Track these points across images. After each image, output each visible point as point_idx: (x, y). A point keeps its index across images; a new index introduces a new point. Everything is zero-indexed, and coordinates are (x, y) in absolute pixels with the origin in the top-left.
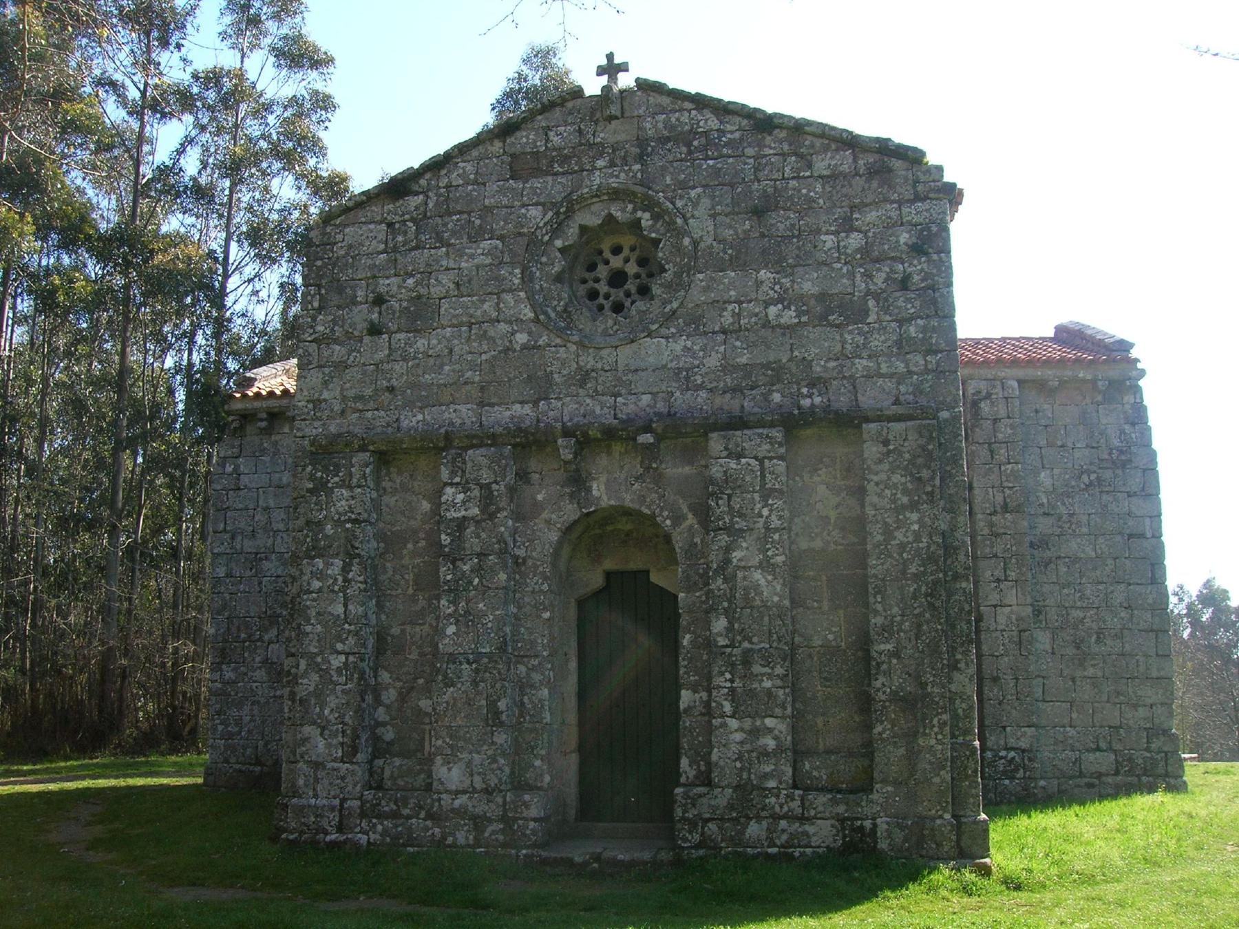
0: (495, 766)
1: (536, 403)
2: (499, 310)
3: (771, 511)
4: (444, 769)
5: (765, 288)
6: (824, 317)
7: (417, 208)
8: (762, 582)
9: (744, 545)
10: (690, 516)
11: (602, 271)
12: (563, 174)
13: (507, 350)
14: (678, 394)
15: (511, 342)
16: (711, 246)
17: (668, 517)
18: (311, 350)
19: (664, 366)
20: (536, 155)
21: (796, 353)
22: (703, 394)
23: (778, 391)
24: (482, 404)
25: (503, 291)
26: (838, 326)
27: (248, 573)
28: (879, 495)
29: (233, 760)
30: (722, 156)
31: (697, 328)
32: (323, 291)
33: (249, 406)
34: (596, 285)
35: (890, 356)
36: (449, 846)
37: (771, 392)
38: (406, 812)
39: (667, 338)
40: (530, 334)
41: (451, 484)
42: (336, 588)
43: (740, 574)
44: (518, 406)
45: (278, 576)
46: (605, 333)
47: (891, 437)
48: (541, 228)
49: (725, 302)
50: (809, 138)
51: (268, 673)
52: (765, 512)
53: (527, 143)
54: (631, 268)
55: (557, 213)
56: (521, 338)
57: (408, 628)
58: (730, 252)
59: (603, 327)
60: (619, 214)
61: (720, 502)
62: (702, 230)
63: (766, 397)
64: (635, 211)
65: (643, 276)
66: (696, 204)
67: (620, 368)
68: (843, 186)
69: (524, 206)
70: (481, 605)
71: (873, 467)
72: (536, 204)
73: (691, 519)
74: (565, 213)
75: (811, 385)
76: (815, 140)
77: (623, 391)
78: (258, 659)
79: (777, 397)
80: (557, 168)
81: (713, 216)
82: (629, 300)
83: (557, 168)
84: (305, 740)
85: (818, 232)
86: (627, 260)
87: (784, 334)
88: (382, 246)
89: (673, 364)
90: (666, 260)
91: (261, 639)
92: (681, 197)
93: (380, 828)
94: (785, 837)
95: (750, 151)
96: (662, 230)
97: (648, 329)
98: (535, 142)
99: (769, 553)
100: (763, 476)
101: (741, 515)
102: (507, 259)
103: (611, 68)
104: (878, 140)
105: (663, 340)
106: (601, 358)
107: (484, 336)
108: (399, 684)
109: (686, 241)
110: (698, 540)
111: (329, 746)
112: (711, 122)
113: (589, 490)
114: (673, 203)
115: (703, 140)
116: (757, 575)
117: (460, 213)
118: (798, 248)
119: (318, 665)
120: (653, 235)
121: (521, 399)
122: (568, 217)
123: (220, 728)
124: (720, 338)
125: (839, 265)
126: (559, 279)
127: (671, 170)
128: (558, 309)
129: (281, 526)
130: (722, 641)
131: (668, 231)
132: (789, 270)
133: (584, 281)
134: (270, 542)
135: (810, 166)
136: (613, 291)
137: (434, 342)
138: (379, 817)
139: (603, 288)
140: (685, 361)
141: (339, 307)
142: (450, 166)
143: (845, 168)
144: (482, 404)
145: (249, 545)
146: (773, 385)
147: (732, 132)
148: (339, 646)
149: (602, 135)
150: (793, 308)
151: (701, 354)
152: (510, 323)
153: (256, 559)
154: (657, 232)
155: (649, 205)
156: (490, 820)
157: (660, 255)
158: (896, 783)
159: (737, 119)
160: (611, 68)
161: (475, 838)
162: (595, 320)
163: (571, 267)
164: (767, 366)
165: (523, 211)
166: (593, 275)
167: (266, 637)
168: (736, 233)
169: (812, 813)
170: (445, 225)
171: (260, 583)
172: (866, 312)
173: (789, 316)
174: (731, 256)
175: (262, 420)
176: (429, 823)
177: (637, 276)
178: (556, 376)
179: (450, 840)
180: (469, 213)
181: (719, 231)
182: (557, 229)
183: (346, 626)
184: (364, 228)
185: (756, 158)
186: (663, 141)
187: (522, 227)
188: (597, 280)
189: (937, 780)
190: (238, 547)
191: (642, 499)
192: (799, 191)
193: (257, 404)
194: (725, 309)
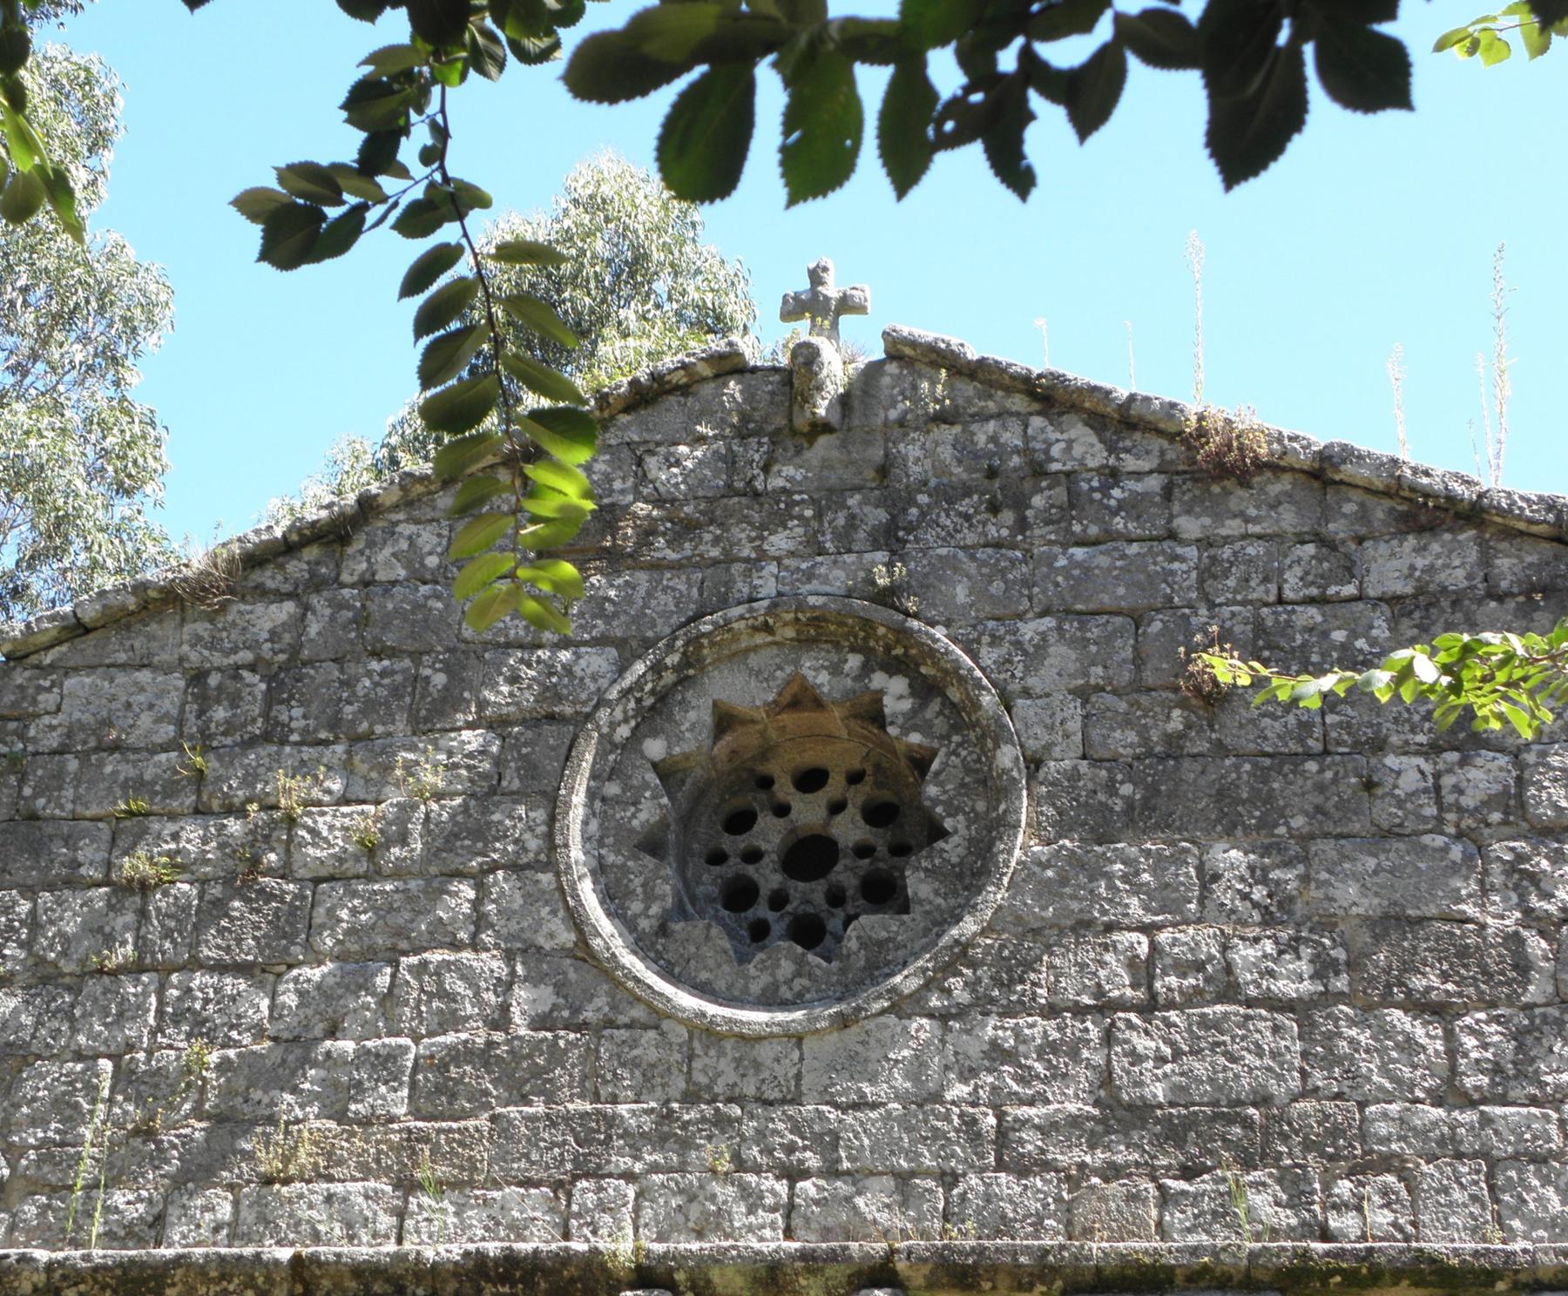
7: (274, 636)
11: (769, 834)
12: (676, 567)
30: (1110, 536)
40: (559, 988)
50: (1356, 495)
54: (849, 830)
55: (657, 668)
58: (1126, 789)
59: (765, 979)
60: (823, 678)
62: (1050, 728)
64: (866, 670)
65: (882, 850)
66: (1035, 655)
72: (600, 642)
74: (677, 669)
76: (1370, 500)
81: (1083, 694)
82: (840, 914)
86: (837, 808)
88: (168, 731)
90: (948, 804)
92: (995, 641)
95: (1190, 526)
96: (940, 725)
98: (608, 479)
102: (512, 782)
106: (757, 1066)
109: (1007, 756)
112: (1078, 446)
114: (975, 657)
115: (1060, 494)
118: (1321, 788)
120: (915, 738)
122: (683, 681)
125: (1440, 841)
126: (652, 845)
127: (972, 567)
128: (644, 924)
131: (956, 728)
133: (717, 858)
135: (1349, 570)
136: (797, 888)
139: (769, 877)
143: (1456, 577)
147: (1138, 475)
149: (789, 470)
150: (1306, 952)
154: (925, 729)
155: (903, 658)
157: (932, 790)
159: (1158, 443)
162: (743, 959)
163: (687, 820)
165: (565, 656)
166: (742, 842)
168: (1145, 740)
170: (349, 684)
174: (1129, 802)
177: (863, 851)
180: (416, 656)
181: (1096, 734)
184: (121, 678)
185: (1205, 543)
186: (948, 494)
187: (559, 698)
188: (753, 856)
192: (1325, 634)
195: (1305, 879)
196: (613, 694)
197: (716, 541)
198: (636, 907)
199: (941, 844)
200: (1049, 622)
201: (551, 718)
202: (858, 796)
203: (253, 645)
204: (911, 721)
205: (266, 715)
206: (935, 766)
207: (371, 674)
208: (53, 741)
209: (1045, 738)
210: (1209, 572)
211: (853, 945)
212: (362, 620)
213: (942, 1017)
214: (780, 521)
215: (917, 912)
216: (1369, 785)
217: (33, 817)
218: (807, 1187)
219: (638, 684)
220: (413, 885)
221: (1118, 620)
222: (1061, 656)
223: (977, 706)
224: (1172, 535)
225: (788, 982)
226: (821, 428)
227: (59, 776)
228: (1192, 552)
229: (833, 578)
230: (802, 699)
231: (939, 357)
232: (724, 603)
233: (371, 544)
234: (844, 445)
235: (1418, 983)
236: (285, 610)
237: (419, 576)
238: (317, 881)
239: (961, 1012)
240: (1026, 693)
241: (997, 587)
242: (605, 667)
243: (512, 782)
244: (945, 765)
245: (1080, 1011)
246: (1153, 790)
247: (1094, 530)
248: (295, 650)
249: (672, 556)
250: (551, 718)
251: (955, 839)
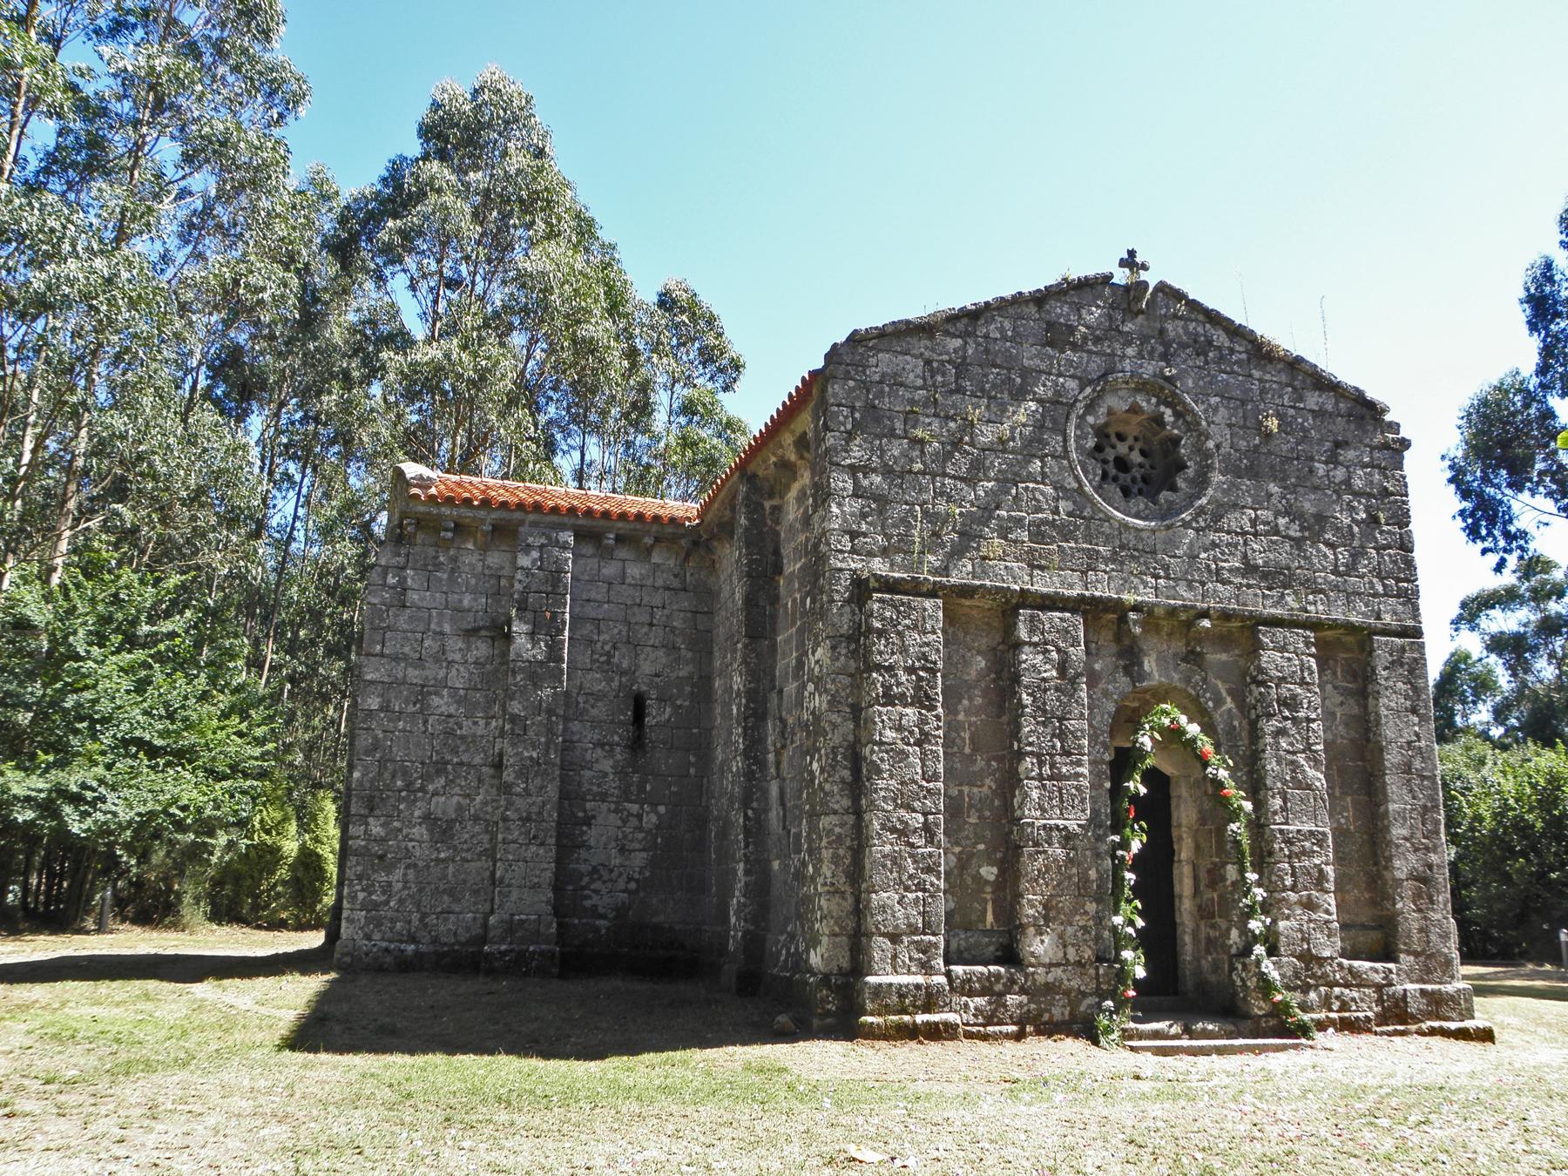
7: (955, 351)
10: (1229, 699)
12: (1096, 353)
27: (411, 709)
29: (377, 936)
30: (1232, 372)
32: (857, 415)
33: (434, 511)
40: (1075, 503)
41: (1030, 644)
45: (450, 716)
51: (431, 831)
54: (1136, 457)
57: (966, 789)
64: (1158, 404)
66: (1216, 410)
73: (1229, 703)
78: (417, 813)
80: (1090, 346)
81: (1230, 426)
84: (883, 908)
85: (1312, 459)
86: (1131, 449)
91: (423, 789)
95: (1256, 374)
102: (1048, 424)
103: (1130, 261)
104: (1357, 389)
108: (957, 850)
110: (1236, 723)
113: (1141, 664)
123: (361, 895)
129: (457, 657)
131: (1189, 430)
134: (442, 674)
135: (1301, 399)
136: (1122, 475)
143: (1329, 407)
145: (414, 675)
153: (422, 694)
155: (1173, 402)
156: (1084, 995)
158: (1416, 954)
160: (1130, 261)
167: (431, 788)
170: (986, 375)
171: (426, 722)
175: (446, 530)
177: (1141, 466)
179: (1046, 1017)
180: (1009, 370)
185: (1260, 380)
186: (1183, 346)
190: (400, 675)
193: (446, 511)
201: (1058, 402)
202: (1138, 446)
203: (948, 353)
204: (1174, 425)
208: (877, 378)
210: (1263, 391)
212: (987, 351)
213: (1197, 530)
214: (1129, 343)
216: (1311, 471)
217: (874, 407)
222: (1222, 411)
223: (1199, 424)
224: (1251, 376)
226: (1141, 312)
227: (882, 392)
229: (1149, 369)
230: (1135, 409)
231: (1178, 295)
236: (958, 342)
237: (1005, 338)
239: (1203, 529)
243: (1048, 424)
248: (964, 358)
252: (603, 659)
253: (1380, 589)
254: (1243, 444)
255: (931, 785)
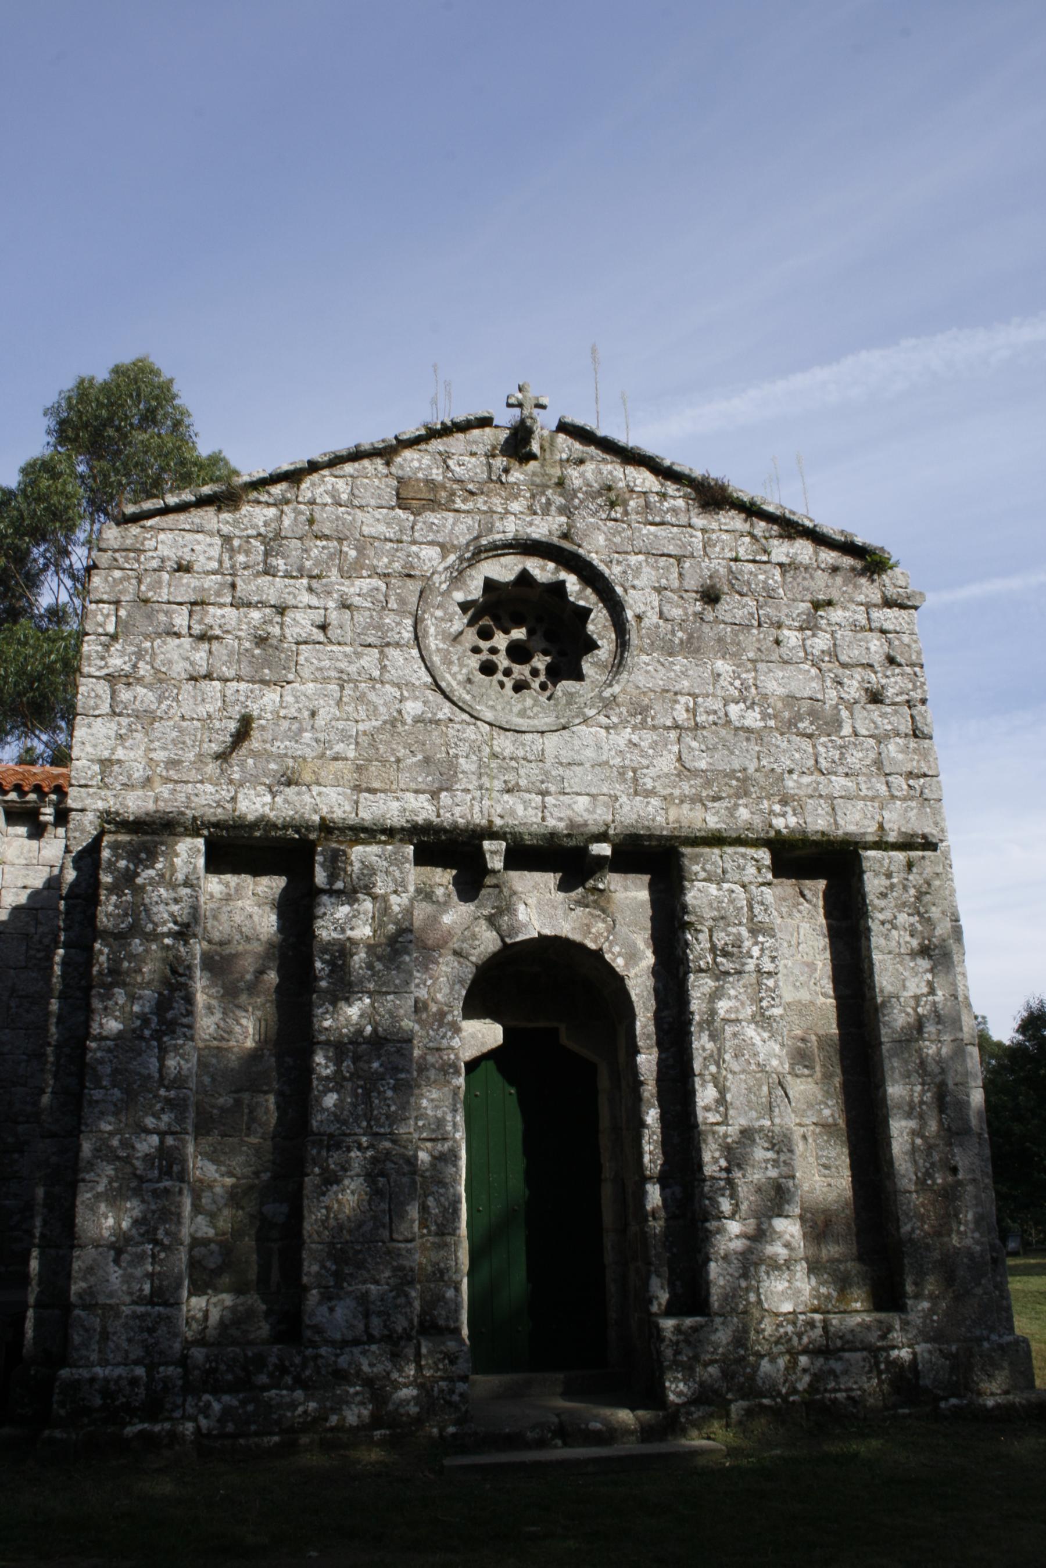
0: (401, 1300)
1: (435, 795)
2: (384, 668)
3: (762, 950)
4: (324, 1309)
5: (722, 682)
6: (792, 723)
8: (757, 1040)
9: (732, 992)
13: (393, 723)
14: (624, 799)
15: (400, 712)
16: (657, 626)
17: (620, 954)
18: (100, 692)
19: (607, 763)
20: (429, 482)
21: (764, 762)
22: (655, 801)
23: (746, 806)
24: (357, 788)
25: (388, 644)
26: (810, 736)
28: (887, 937)
31: (644, 721)
32: (122, 613)
34: (494, 657)
35: (869, 776)
36: (332, 1429)
37: (736, 806)
38: (263, 1379)
39: (607, 728)
42: (147, 1033)
43: (729, 1030)
44: (410, 796)
46: (522, 714)
47: (892, 868)
48: (440, 573)
49: (676, 694)
52: (756, 951)
53: (420, 468)
55: (461, 559)
56: (412, 708)
57: (246, 1096)
58: (680, 634)
59: (520, 706)
61: (701, 936)
62: (645, 604)
63: (732, 811)
66: (637, 571)
67: (550, 760)
68: (804, 579)
69: (414, 542)
70: (375, 1065)
71: (876, 902)
72: (431, 543)
74: (469, 559)
75: (784, 802)
77: (553, 789)
79: (743, 814)
81: (659, 590)
83: (459, 504)
87: (748, 739)
89: (617, 761)
90: (599, 634)
92: (619, 563)
93: (216, 1407)
94: (807, 1379)
97: (584, 714)
98: (430, 467)
99: (764, 1004)
100: (751, 908)
101: (725, 954)
105: (603, 731)
106: (524, 745)
107: (361, 698)
111: (127, 1278)
115: (642, 501)
116: (750, 1031)
117: (327, 537)
118: (758, 640)
119: (112, 1150)
120: (582, 603)
121: (413, 786)
124: (673, 735)
125: (807, 667)
127: (605, 529)
130: (713, 1118)
132: (750, 666)
136: (516, 668)
137: (289, 699)
138: (216, 1391)
140: (633, 758)
141: (147, 637)
142: (315, 477)
144: (357, 788)
146: (739, 798)
147: (674, 498)
148: (150, 1122)
150: (757, 709)
151: (651, 752)
152: (398, 686)
154: (586, 599)
161: (372, 1415)
164: (731, 774)
168: (686, 614)
169: (839, 1343)
172: (839, 724)
173: (753, 719)
176: (299, 1394)
178: (462, 761)
179: (334, 1420)
180: (340, 540)
181: (665, 609)
182: (457, 578)
183: (162, 1092)
185: (704, 531)
189: (979, 1291)
191: (587, 929)
192: (756, 576)
194: (676, 702)
195: (755, 679)
196: (440, 568)
197: (486, 502)
198: (455, 669)
199: (596, 652)
200: (641, 557)
201: (409, 576)
203: (255, 526)
205: (265, 562)
206: (592, 616)
207: (317, 549)
208: (155, 564)
209: (643, 609)
211: (560, 694)
212: (311, 521)
214: (516, 497)
215: (588, 680)
216: (778, 642)
217: (146, 601)
218: (549, 800)
219: (452, 566)
220: (348, 649)
221: (672, 560)
225: (531, 709)
227: (159, 582)
228: (699, 534)
232: (490, 531)
233: (313, 484)
234: (543, 466)
235: (800, 725)
236: (272, 512)
238: (298, 643)
239: (615, 726)
240: (634, 587)
241: (617, 540)
242: (435, 556)
243: (393, 604)
244: (597, 616)
245: (669, 728)
246: (691, 637)
247: (658, 519)
249: (464, 507)
250: (409, 576)
251: (603, 650)
252: (40, 955)
253: (883, 789)
254: (676, 613)
255: (172, 1094)
